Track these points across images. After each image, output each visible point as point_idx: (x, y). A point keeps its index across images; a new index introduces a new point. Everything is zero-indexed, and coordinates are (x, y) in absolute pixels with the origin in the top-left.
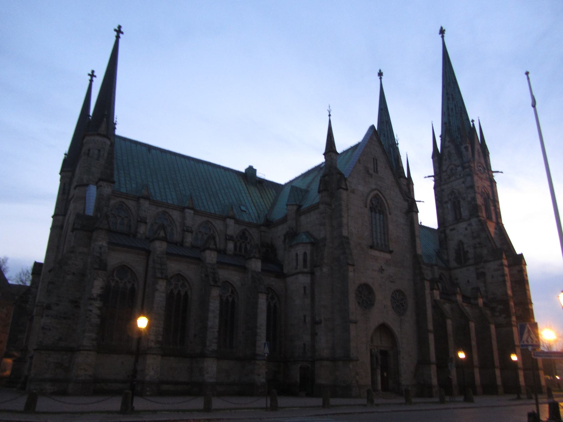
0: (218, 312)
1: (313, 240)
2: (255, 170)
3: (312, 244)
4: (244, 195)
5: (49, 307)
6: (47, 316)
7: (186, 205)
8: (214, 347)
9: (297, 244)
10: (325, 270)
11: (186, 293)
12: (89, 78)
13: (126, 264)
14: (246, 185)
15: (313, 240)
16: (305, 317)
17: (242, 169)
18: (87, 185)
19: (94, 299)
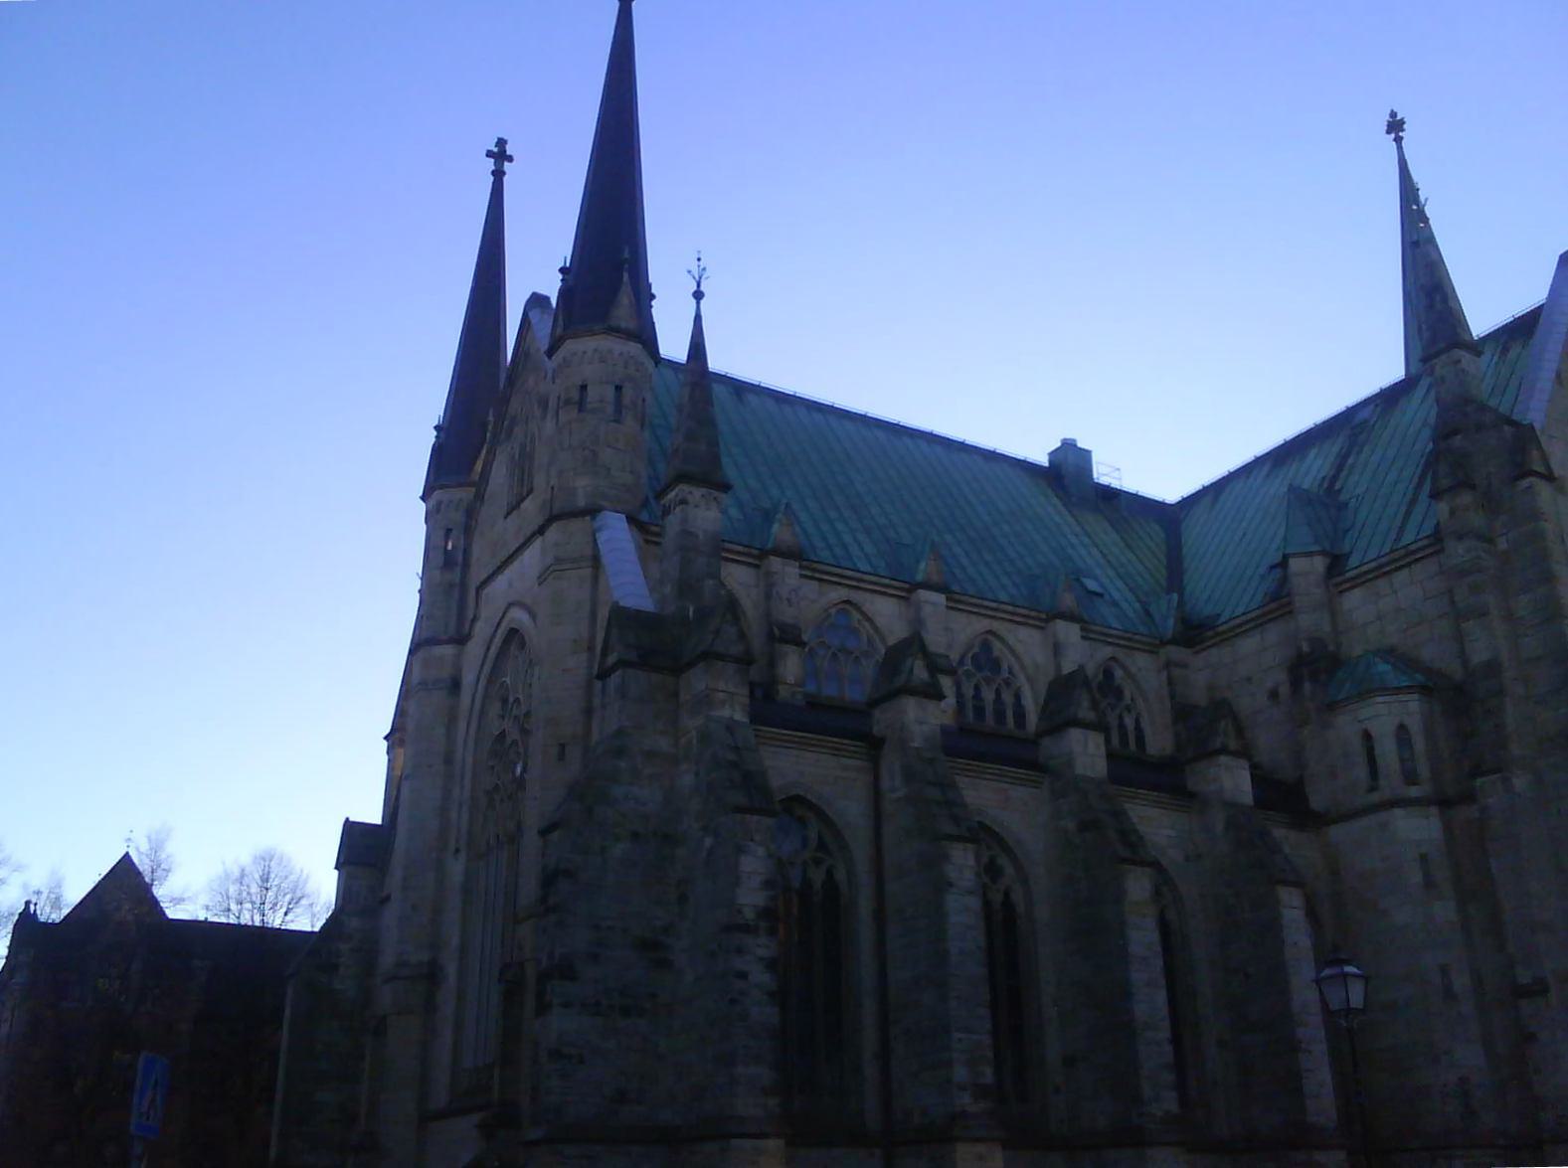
0: (1160, 963)
1: (1419, 677)
2: (1086, 455)
3: (1425, 690)
4: (1074, 540)
5: (565, 970)
6: (566, 1005)
7: (920, 577)
8: (1170, 1103)
9: (1365, 694)
10: (1520, 782)
11: (1007, 894)
12: (490, 163)
13: (802, 793)
14: (1065, 505)
15: (1419, 677)
16: (1444, 970)
17: (1039, 454)
18: (592, 512)
19: (747, 929)
